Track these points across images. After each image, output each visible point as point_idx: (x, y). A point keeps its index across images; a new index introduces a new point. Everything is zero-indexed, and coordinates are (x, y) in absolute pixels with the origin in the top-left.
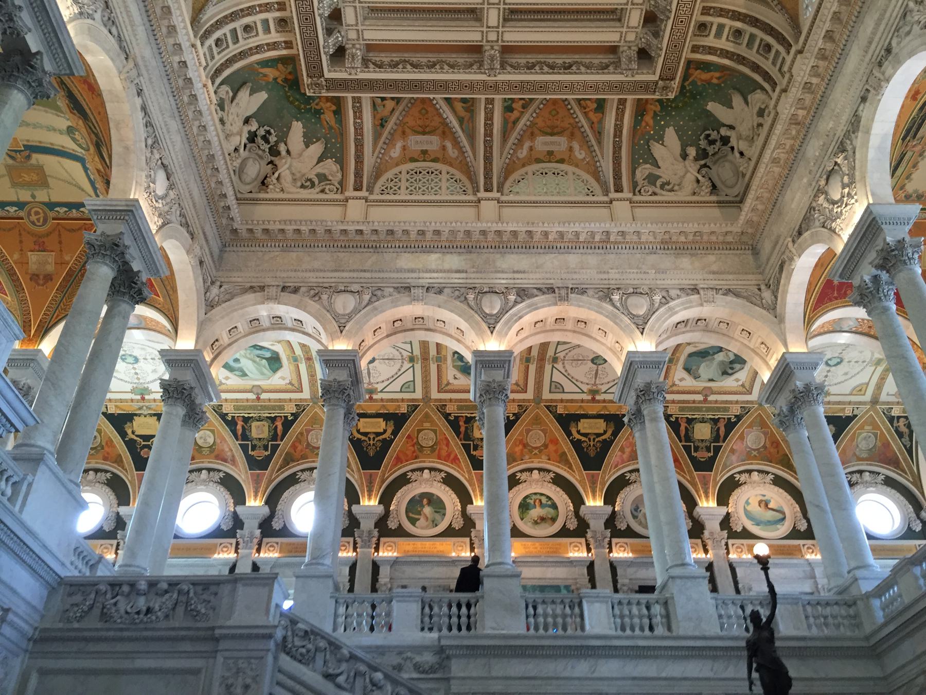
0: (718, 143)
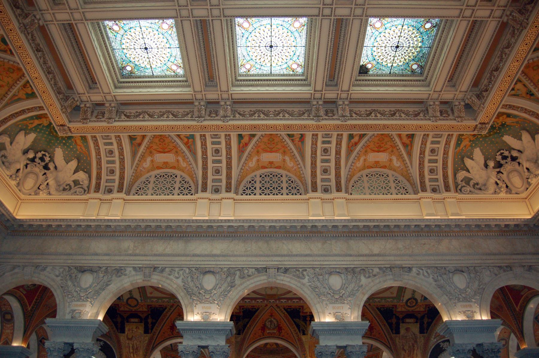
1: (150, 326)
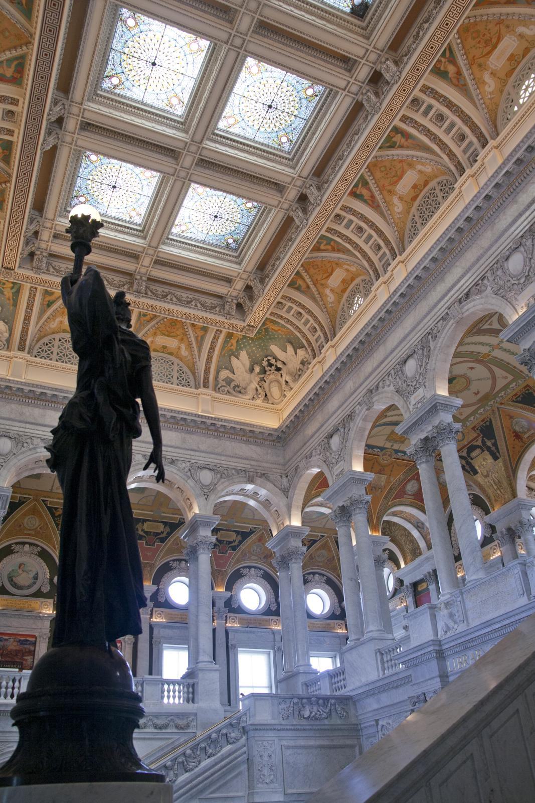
0: (274, 368)
1: (493, 449)
